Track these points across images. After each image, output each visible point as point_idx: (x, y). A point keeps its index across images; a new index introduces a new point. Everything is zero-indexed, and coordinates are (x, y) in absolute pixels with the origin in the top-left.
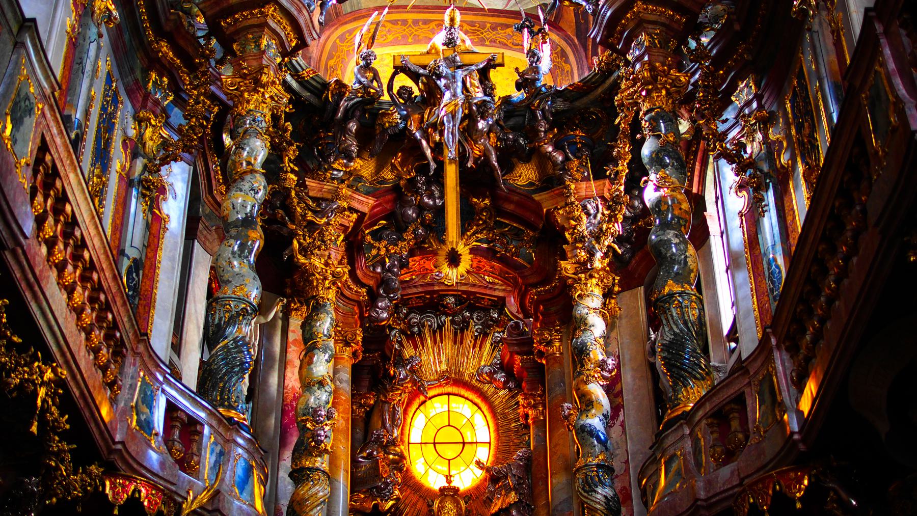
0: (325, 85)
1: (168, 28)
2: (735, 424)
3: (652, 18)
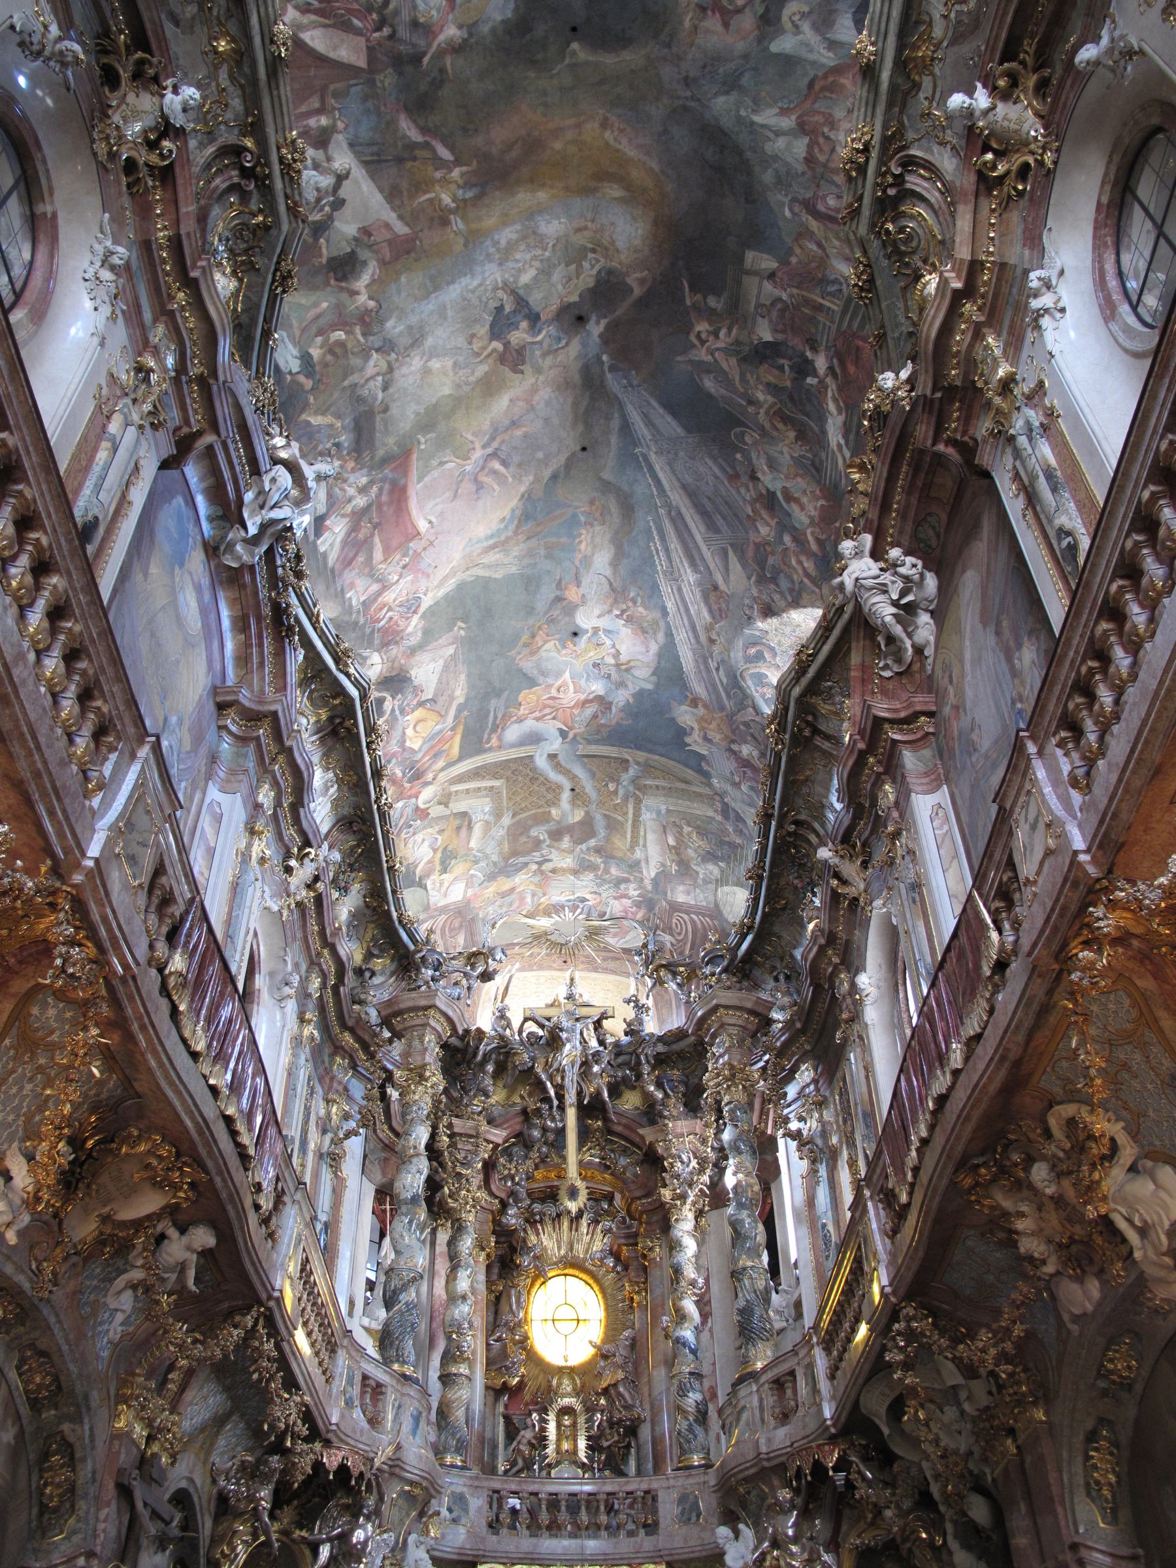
0: (467, 1031)
1: (350, 1023)
2: (789, 1392)
3: (732, 1021)
